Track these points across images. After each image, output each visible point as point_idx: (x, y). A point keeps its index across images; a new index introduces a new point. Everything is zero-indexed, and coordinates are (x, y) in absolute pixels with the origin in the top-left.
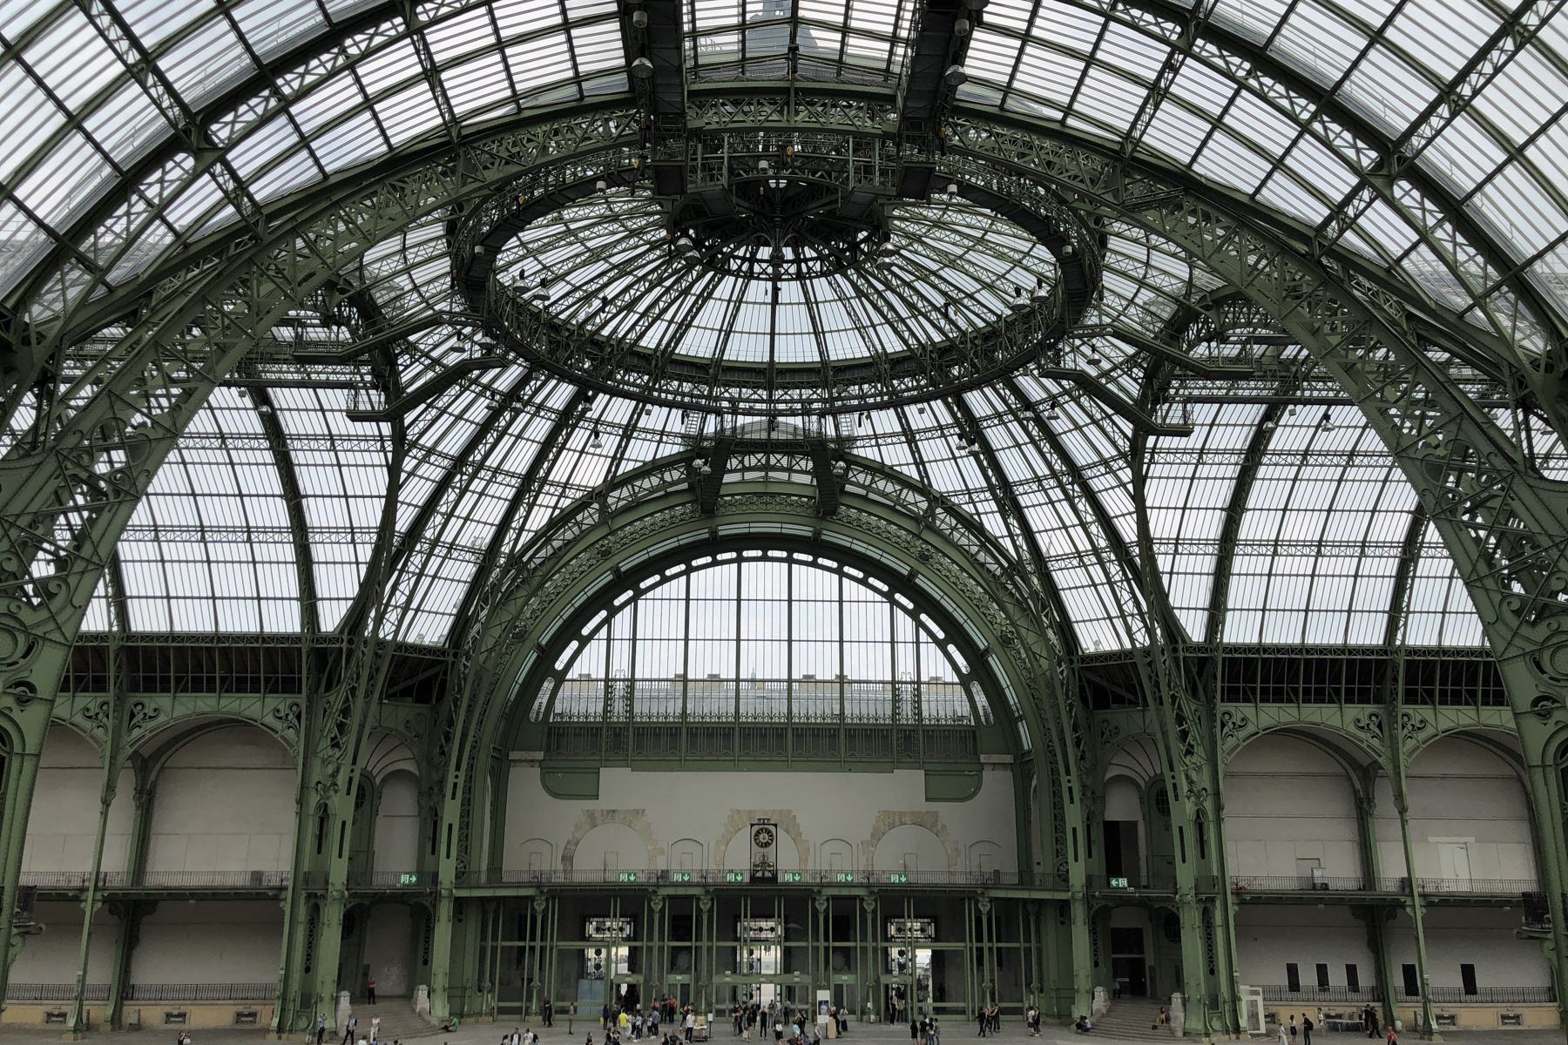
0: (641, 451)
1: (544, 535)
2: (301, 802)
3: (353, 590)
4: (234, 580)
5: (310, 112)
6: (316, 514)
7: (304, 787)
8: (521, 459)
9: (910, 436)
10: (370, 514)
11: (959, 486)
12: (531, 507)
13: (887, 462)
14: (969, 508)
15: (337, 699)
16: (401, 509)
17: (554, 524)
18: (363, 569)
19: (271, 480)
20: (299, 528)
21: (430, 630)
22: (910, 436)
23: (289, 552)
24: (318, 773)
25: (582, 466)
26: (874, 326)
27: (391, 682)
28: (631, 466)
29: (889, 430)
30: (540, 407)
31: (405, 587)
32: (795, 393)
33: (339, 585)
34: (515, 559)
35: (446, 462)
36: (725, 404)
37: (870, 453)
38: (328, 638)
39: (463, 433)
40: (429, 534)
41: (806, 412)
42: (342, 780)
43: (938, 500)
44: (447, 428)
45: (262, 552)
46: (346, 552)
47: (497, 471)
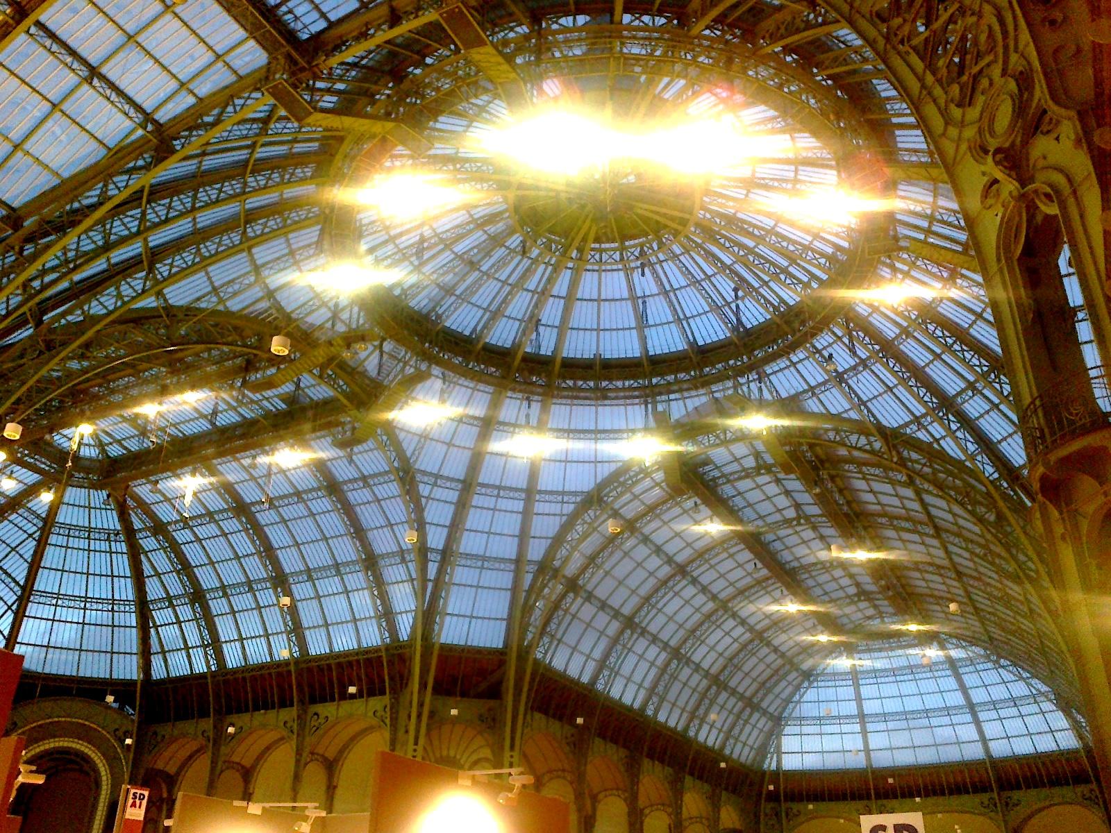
13: (833, 411)
14: (922, 435)
20: (370, 562)
21: (489, 636)
26: (766, 283)
29: (821, 380)
33: (404, 599)
43: (893, 437)
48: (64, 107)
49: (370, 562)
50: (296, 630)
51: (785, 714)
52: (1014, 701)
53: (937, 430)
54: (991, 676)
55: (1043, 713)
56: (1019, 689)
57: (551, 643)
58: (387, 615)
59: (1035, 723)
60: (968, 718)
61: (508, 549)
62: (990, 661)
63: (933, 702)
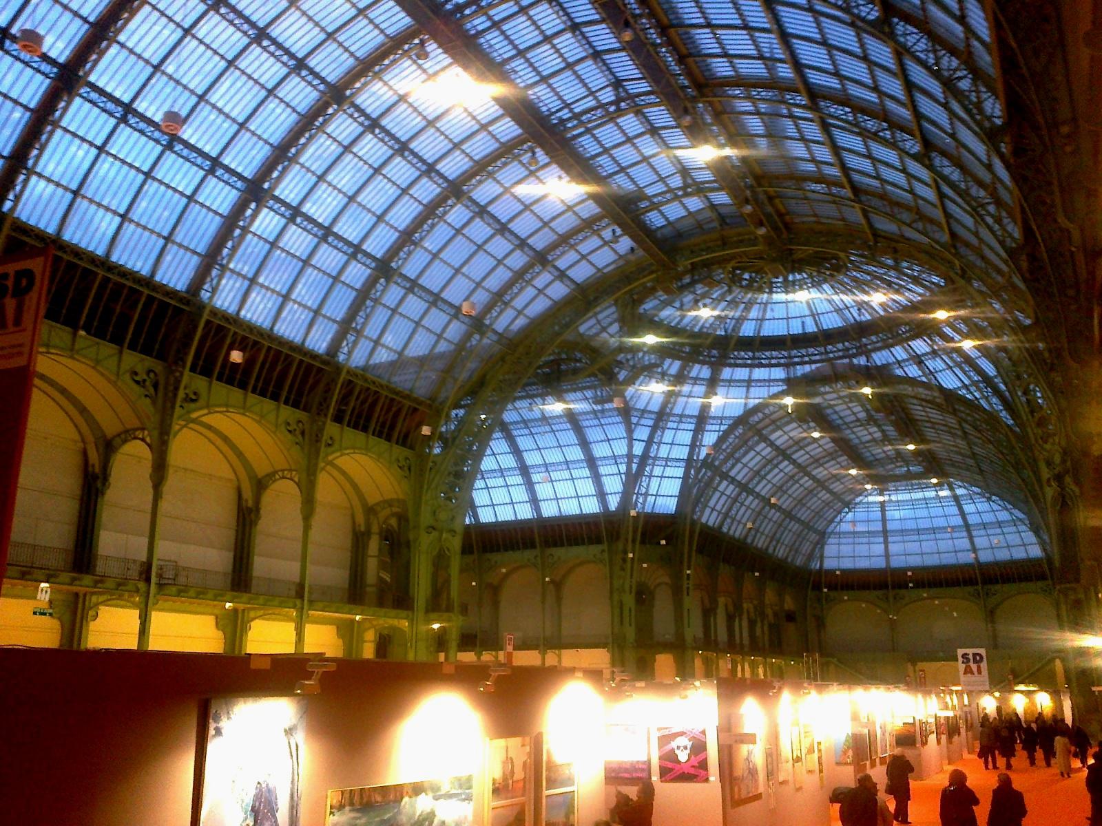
1: (717, 446)
2: (611, 598)
4: (564, 489)
5: (519, 303)
6: (600, 451)
7: (611, 592)
9: (919, 360)
12: (703, 430)
13: (911, 375)
15: (620, 545)
16: (636, 444)
17: (721, 440)
18: (623, 476)
22: (919, 360)
24: (616, 583)
27: (643, 534)
31: (644, 484)
32: (840, 346)
33: (613, 485)
35: (653, 416)
36: (796, 360)
37: (899, 372)
42: (627, 587)
43: (949, 395)
45: (576, 473)
46: (614, 469)
48: (545, 292)
49: (591, 462)
50: (534, 501)
51: (830, 530)
52: (1000, 524)
54: (983, 506)
55: (1019, 532)
56: (1004, 516)
57: (732, 523)
58: (601, 495)
59: (1014, 539)
60: (965, 534)
61: (683, 453)
62: (984, 497)
63: (941, 522)
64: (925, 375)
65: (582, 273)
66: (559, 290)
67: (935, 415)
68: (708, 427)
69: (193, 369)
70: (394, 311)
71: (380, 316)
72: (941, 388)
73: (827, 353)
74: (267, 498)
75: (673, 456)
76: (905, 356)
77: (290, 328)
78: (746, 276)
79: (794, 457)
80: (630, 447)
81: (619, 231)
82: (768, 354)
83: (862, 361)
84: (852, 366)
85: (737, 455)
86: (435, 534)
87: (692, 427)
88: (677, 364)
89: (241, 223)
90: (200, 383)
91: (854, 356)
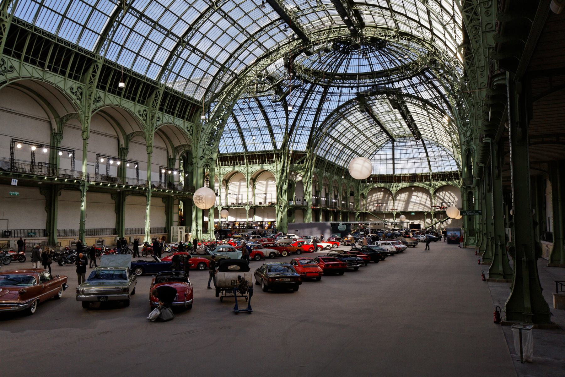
0: (345, 99)
3: (282, 139)
5: (241, 58)
6: (273, 123)
8: (316, 104)
9: (413, 86)
10: (283, 122)
11: (430, 98)
16: (290, 120)
17: (327, 119)
19: (260, 116)
21: (302, 147)
23: (268, 132)
25: (332, 105)
28: (343, 103)
30: (317, 92)
31: (293, 138)
32: (381, 79)
34: (320, 129)
36: (362, 84)
38: (279, 150)
39: (300, 101)
40: (297, 125)
41: (385, 84)
44: (295, 100)
46: (280, 131)
47: (310, 108)
53: (438, 102)
59: (447, 163)
61: (310, 124)
63: (417, 155)
64: (416, 93)
65: (270, 45)
66: (260, 52)
67: (419, 110)
68: (322, 114)
69: (97, 87)
70: (186, 61)
71: (180, 62)
72: (422, 100)
73: (375, 82)
74: (131, 145)
75: (306, 125)
76: (408, 84)
77: (140, 69)
78: (342, 46)
79: (358, 127)
80: (287, 121)
81: (287, 26)
82: (349, 81)
83: (390, 86)
84: (385, 87)
85: (333, 126)
86: (204, 160)
87: (315, 113)
88: (309, 85)
89: (117, 19)
90: (101, 93)
91: (387, 83)
